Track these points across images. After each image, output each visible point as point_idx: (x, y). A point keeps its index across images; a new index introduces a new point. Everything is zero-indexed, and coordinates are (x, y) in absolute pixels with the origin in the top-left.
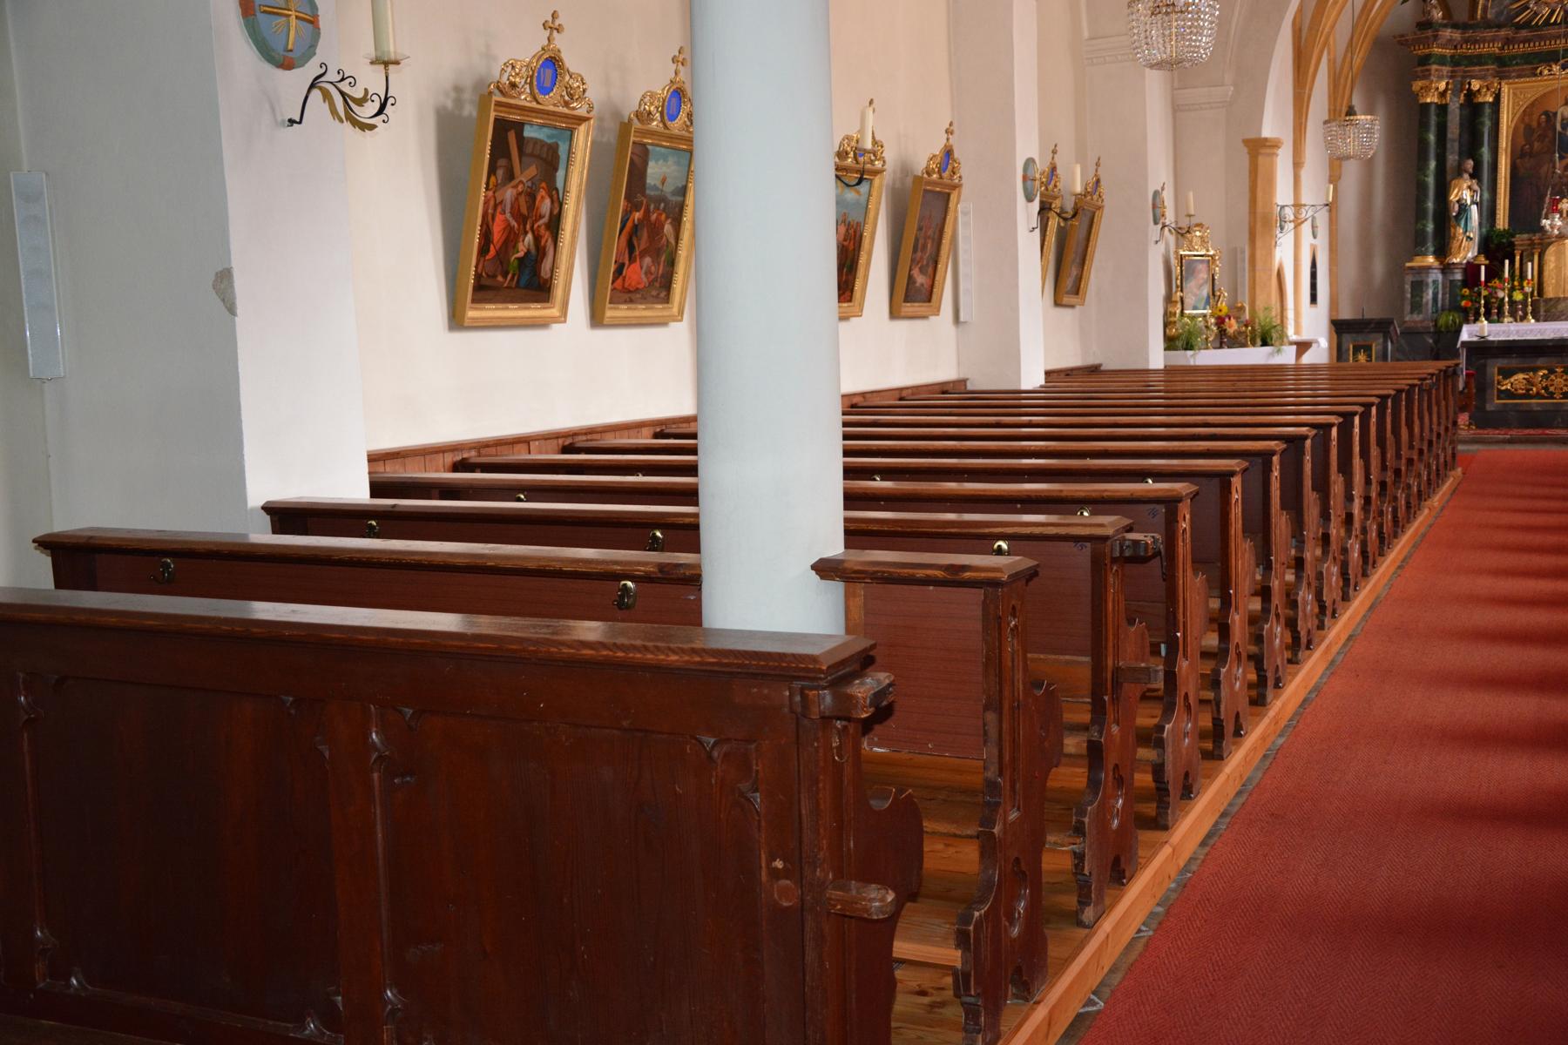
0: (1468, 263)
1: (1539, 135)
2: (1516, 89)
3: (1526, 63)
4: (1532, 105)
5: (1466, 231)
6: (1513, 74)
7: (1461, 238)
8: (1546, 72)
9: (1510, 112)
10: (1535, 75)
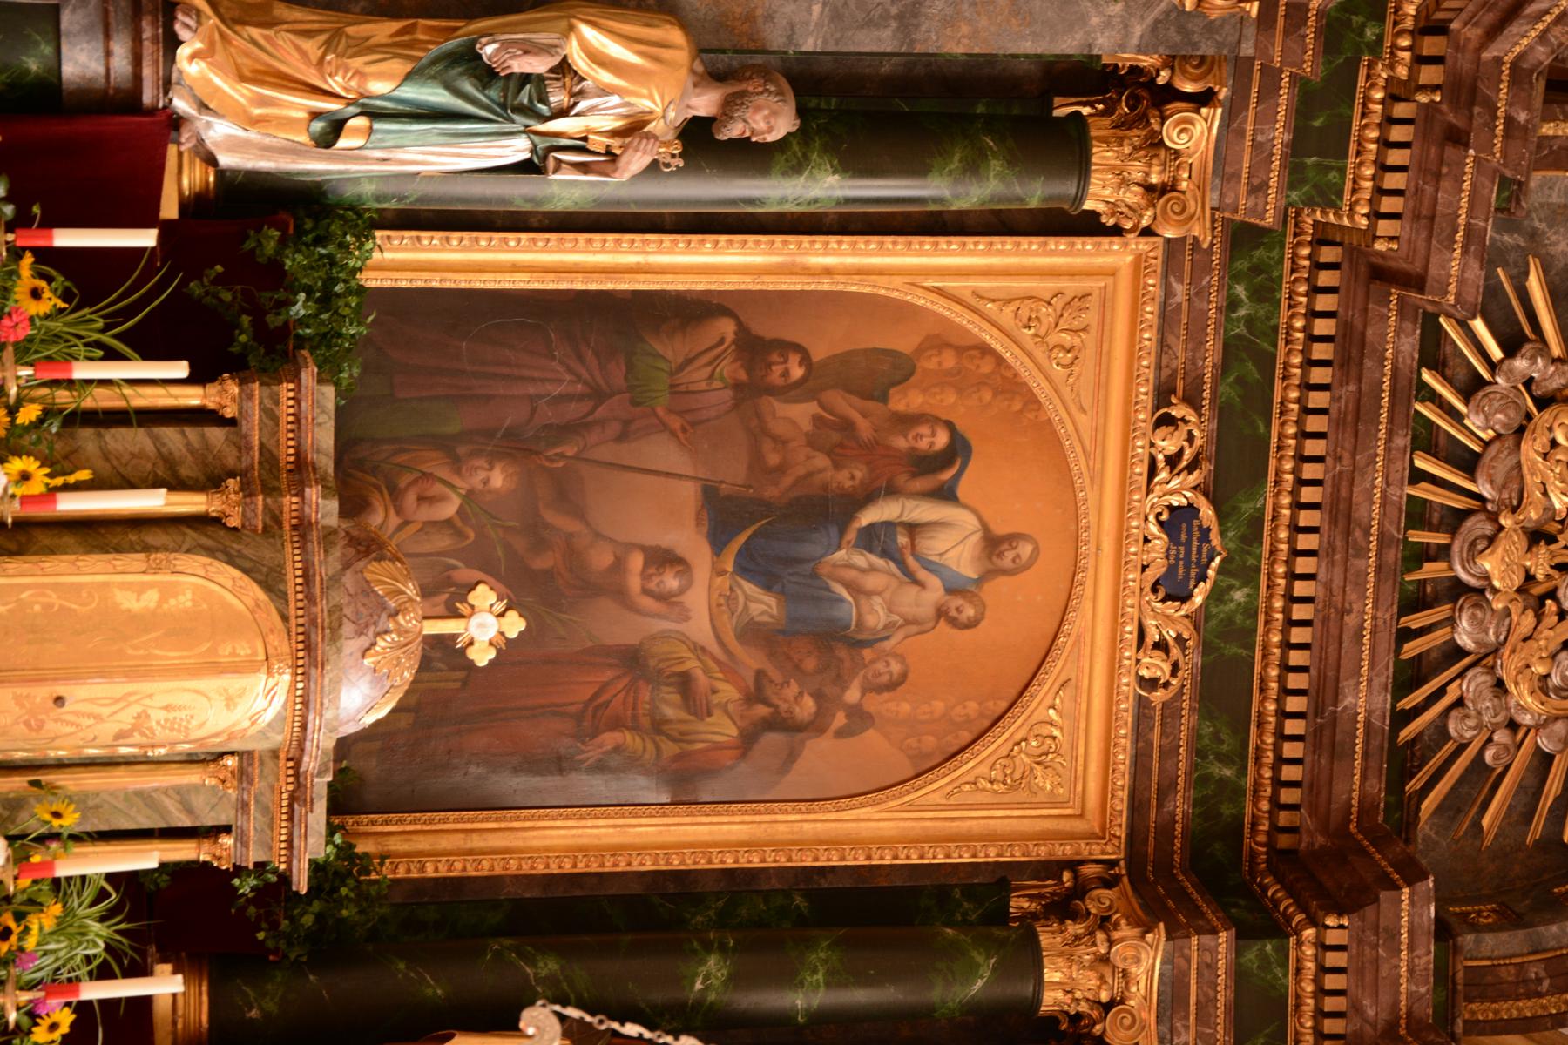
0: (176, 122)
1: (847, 426)
2: (1106, 302)
3: (1231, 350)
4: (1009, 385)
5: (375, 115)
6: (1180, 290)
7: (336, 84)
8: (1168, 444)
9: (982, 284)
10: (1163, 394)
